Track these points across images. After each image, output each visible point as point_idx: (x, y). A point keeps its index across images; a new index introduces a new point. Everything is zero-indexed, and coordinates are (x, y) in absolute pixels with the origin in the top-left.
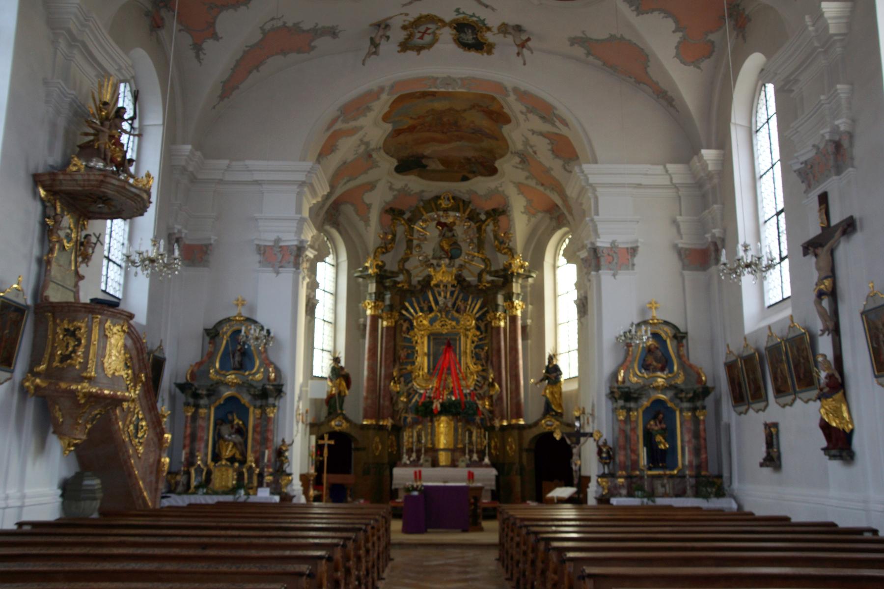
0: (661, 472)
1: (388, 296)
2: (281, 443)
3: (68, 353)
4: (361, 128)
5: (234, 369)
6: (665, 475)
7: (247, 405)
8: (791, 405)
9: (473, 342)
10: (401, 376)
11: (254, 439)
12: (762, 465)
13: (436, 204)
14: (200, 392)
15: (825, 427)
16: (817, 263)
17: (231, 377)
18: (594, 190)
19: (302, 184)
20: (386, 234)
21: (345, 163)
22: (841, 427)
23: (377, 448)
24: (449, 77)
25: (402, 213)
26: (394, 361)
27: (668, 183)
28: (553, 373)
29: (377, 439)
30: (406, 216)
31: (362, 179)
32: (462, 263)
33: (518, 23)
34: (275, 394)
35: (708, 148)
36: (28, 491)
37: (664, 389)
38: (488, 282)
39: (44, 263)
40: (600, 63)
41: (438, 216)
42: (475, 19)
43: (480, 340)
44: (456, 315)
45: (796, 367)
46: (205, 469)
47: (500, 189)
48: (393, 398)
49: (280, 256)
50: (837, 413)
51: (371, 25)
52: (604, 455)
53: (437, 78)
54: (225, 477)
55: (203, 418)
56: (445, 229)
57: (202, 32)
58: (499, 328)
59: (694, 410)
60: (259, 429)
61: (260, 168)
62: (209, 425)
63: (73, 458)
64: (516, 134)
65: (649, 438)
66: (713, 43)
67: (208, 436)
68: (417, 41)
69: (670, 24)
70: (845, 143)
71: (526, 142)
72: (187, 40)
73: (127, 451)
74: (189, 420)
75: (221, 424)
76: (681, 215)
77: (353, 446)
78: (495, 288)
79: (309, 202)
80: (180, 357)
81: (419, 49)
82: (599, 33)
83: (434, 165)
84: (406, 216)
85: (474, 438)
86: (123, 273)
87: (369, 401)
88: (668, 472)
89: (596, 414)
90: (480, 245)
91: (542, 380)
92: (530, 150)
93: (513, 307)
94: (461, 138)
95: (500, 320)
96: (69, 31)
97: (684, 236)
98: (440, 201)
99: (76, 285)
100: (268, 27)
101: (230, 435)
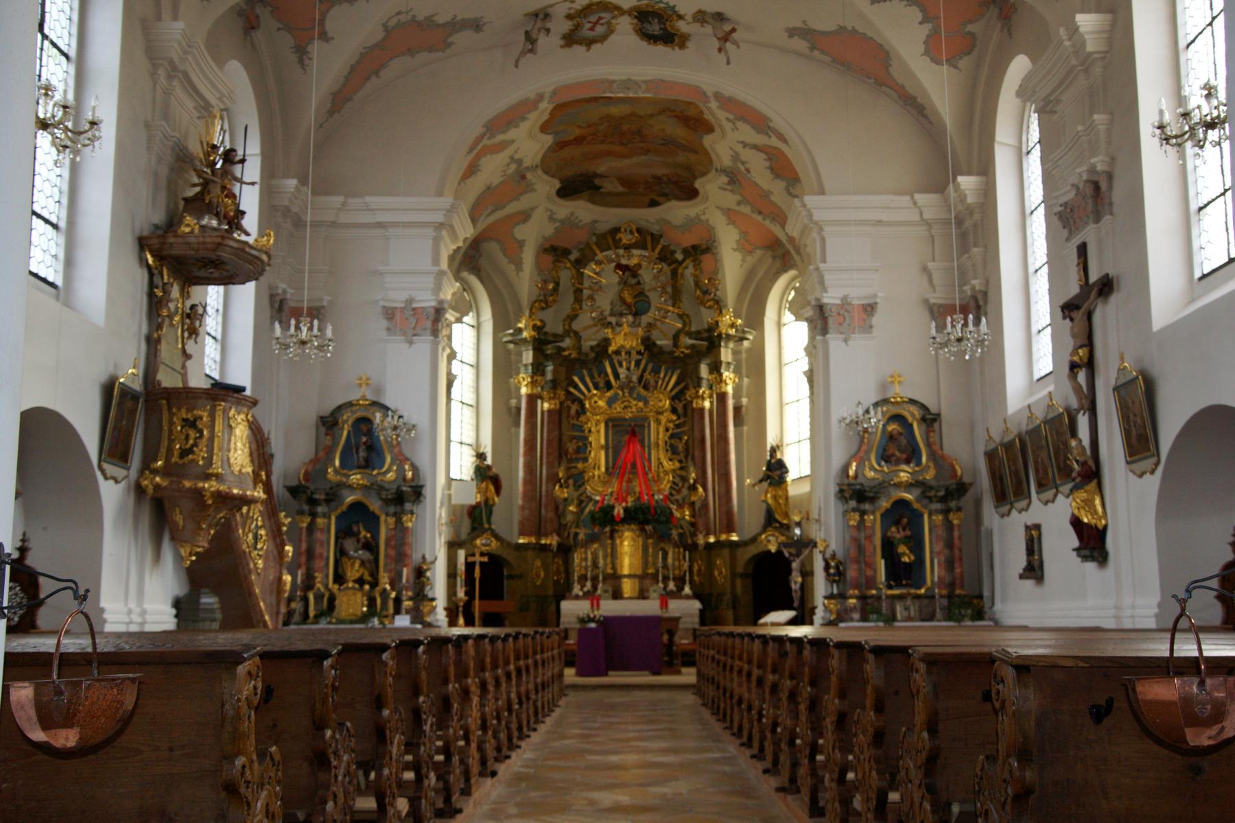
0: (904, 591)
1: (550, 369)
2: (420, 560)
3: (188, 446)
4: (512, 142)
5: (359, 467)
6: (909, 594)
7: (377, 512)
8: (1053, 501)
9: (667, 430)
11: (387, 556)
12: (1021, 577)
13: (614, 239)
14: (317, 496)
15: (1076, 523)
16: (1072, 329)
17: (356, 478)
18: (821, 229)
19: (440, 226)
20: (545, 282)
21: (489, 188)
22: (1093, 522)
23: (538, 576)
24: (629, 80)
25: (566, 252)
26: (560, 456)
27: (918, 218)
28: (776, 471)
29: (538, 563)
30: (573, 257)
31: (512, 208)
32: (651, 320)
33: (719, 10)
34: (413, 498)
35: (969, 173)
36: (147, 606)
37: (909, 486)
38: (687, 348)
39: (152, 343)
40: (827, 59)
41: (618, 256)
42: (662, 5)
43: (677, 426)
45: (1056, 454)
46: (327, 595)
47: (703, 218)
48: (558, 508)
49: (413, 321)
50: (1089, 504)
51: (526, 15)
53: (614, 81)
54: (352, 603)
55: (322, 530)
56: (627, 273)
57: (306, 32)
58: (702, 409)
59: (946, 512)
60: (393, 543)
61: (383, 206)
62: (329, 538)
63: (184, 576)
64: (725, 144)
66: (972, 35)
67: (328, 551)
68: (585, 32)
69: (916, 14)
70: (1104, 186)
71: (736, 157)
72: (286, 41)
73: (248, 564)
74: (304, 534)
75: (344, 538)
76: (934, 260)
77: (505, 573)
78: (696, 355)
79: (448, 247)
80: (292, 455)
81: (589, 43)
82: (824, 22)
83: (610, 186)
84: (573, 257)
85: (670, 560)
86: (219, 347)
87: (527, 512)
88: (913, 591)
89: (823, 519)
90: (676, 297)
91: (761, 481)
92: (742, 168)
93: (721, 380)
94: (647, 152)
95: (703, 399)
96: (171, 62)
97: (937, 289)
98: (619, 236)
99: (184, 367)
100: (393, 22)
101: (356, 551)
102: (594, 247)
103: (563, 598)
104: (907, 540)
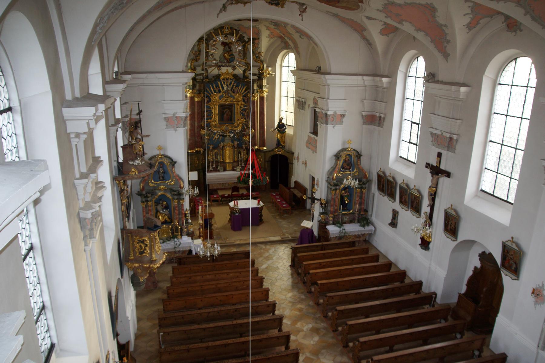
13: (221, 31)
29: (196, 159)
44: (233, 94)
49: (176, 122)
52: (323, 206)
56: (226, 47)
65: (342, 197)
93: (262, 92)
104: (348, 196)
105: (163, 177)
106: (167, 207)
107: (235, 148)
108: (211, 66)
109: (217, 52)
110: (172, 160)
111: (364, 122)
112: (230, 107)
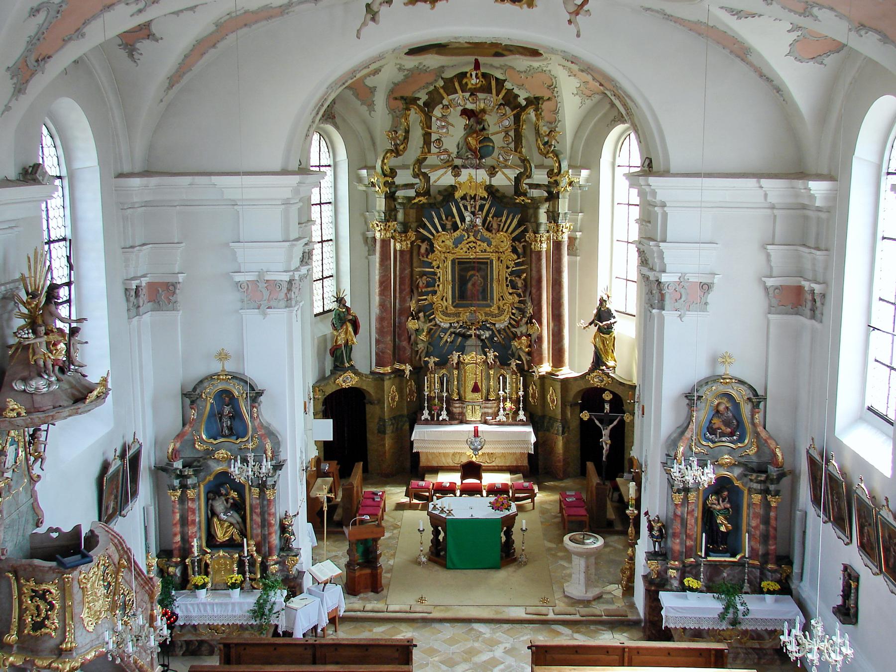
10: (419, 312)
30: (421, 103)
32: (494, 163)
43: (517, 264)
44: (487, 234)
52: (656, 533)
55: (193, 500)
58: (539, 252)
65: (708, 516)
75: (214, 499)
78: (535, 204)
91: (590, 324)
102: (442, 91)
103: (414, 419)
105: (230, 429)
106: (238, 507)
107: (489, 367)
108: (434, 168)
109: (453, 132)
110: (252, 388)
111: (770, 306)
112: (482, 266)
